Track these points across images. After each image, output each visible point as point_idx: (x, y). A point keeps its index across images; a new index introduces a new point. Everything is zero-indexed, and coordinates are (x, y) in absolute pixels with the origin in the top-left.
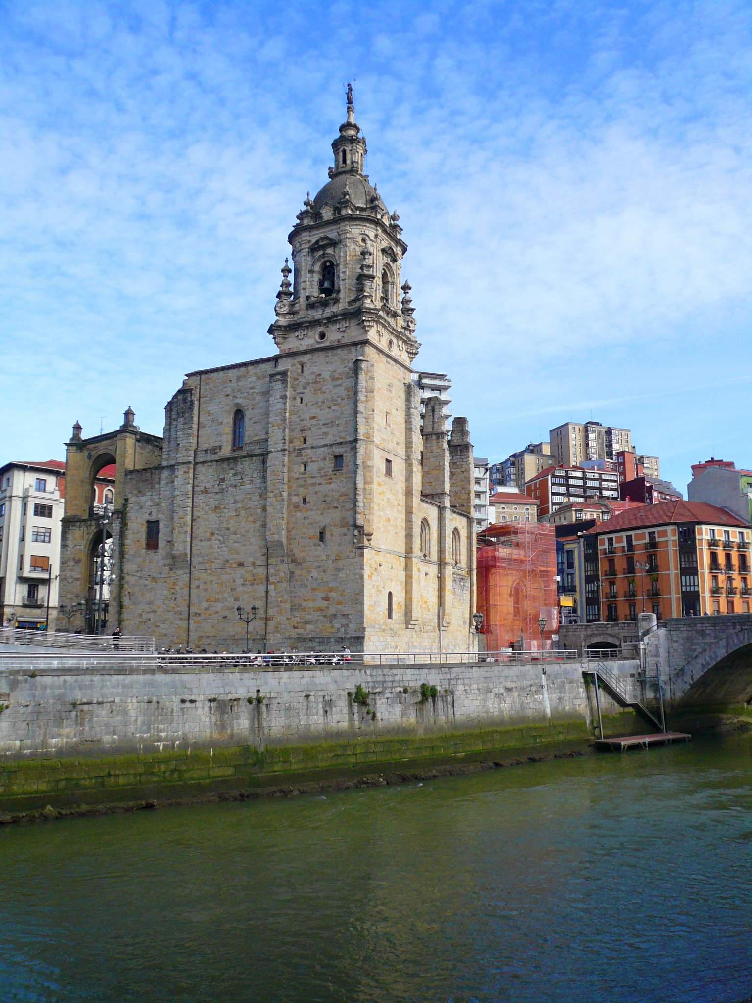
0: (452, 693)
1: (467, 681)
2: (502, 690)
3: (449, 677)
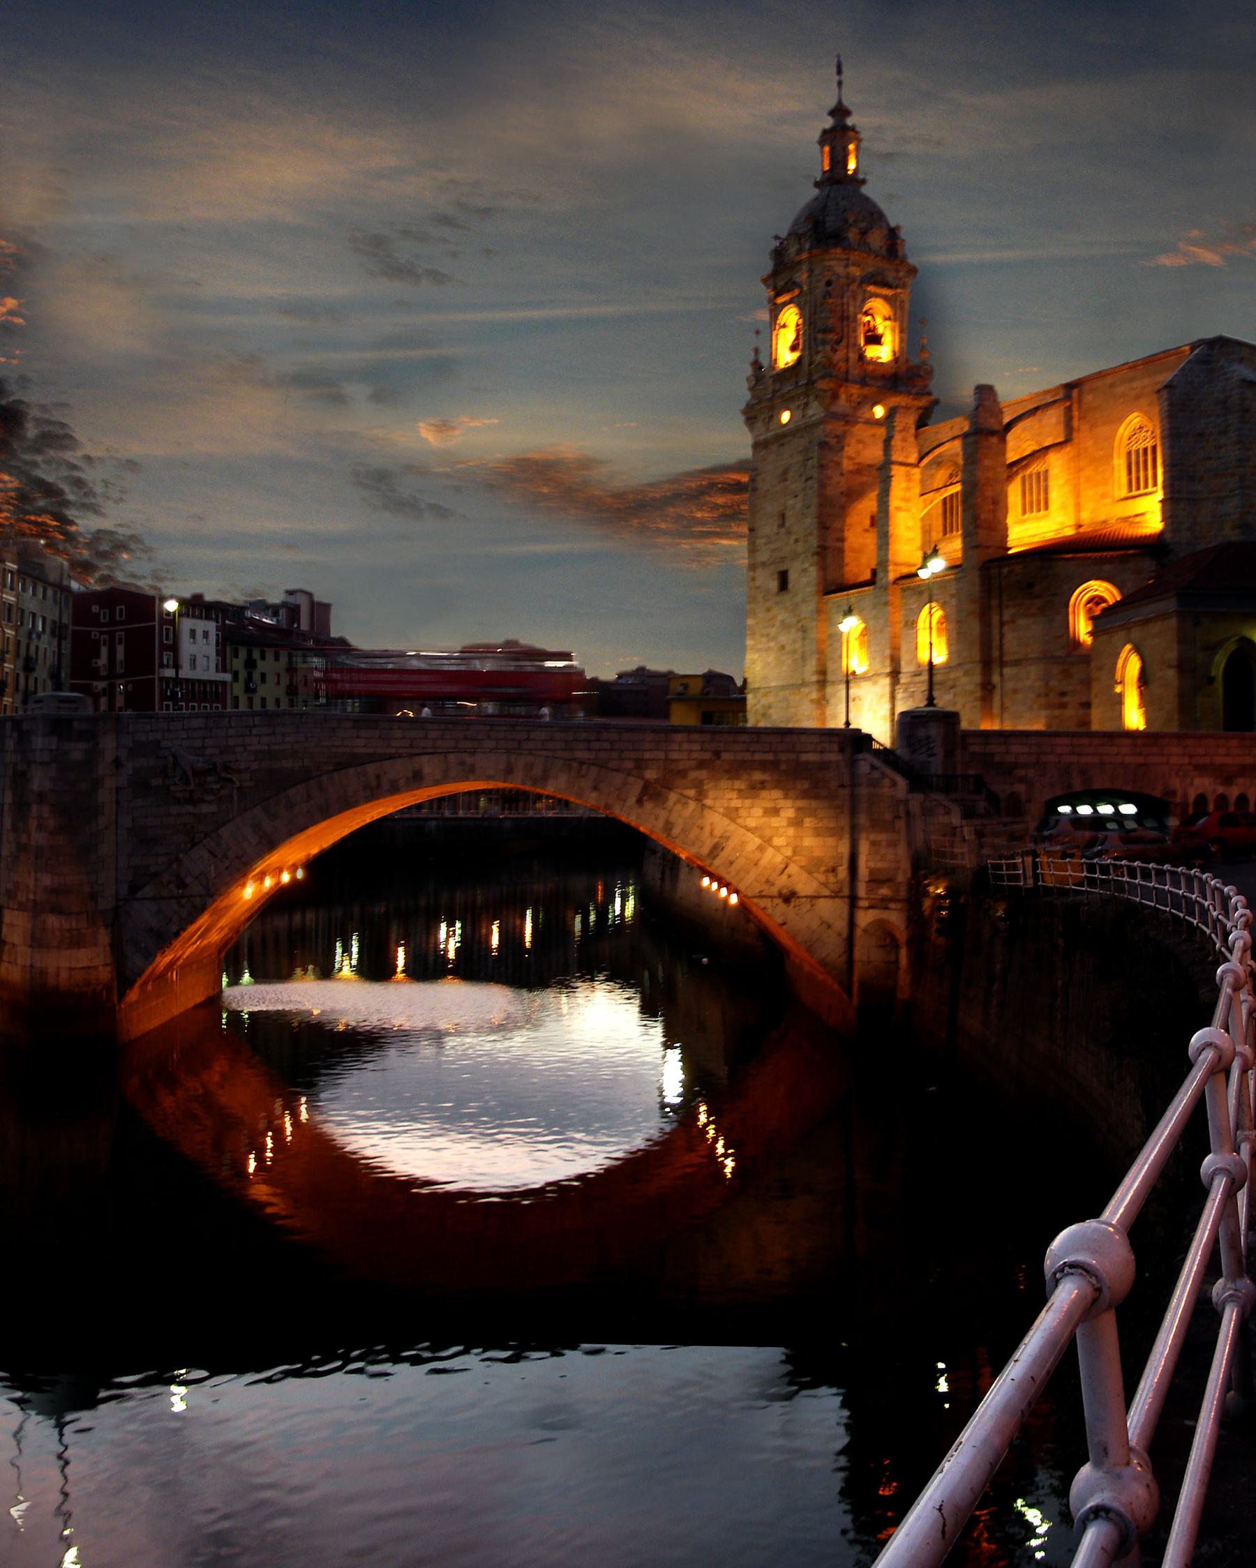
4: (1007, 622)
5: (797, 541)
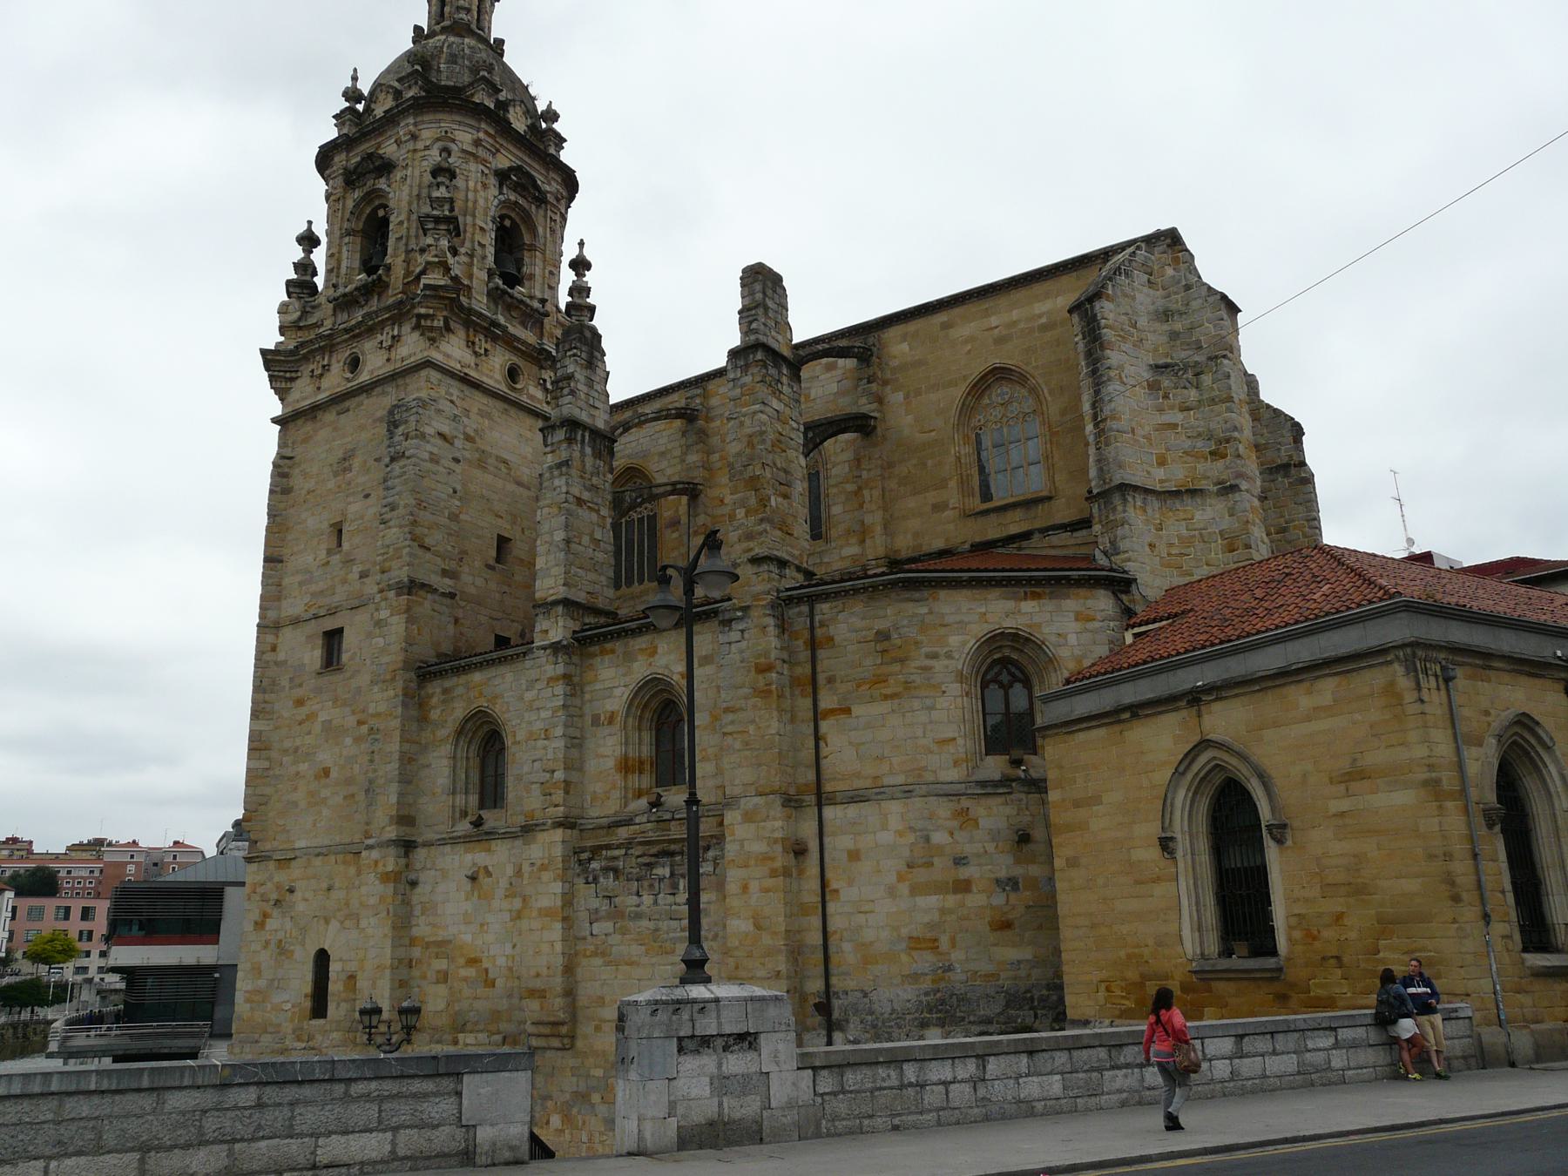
4: (832, 712)
5: (364, 575)
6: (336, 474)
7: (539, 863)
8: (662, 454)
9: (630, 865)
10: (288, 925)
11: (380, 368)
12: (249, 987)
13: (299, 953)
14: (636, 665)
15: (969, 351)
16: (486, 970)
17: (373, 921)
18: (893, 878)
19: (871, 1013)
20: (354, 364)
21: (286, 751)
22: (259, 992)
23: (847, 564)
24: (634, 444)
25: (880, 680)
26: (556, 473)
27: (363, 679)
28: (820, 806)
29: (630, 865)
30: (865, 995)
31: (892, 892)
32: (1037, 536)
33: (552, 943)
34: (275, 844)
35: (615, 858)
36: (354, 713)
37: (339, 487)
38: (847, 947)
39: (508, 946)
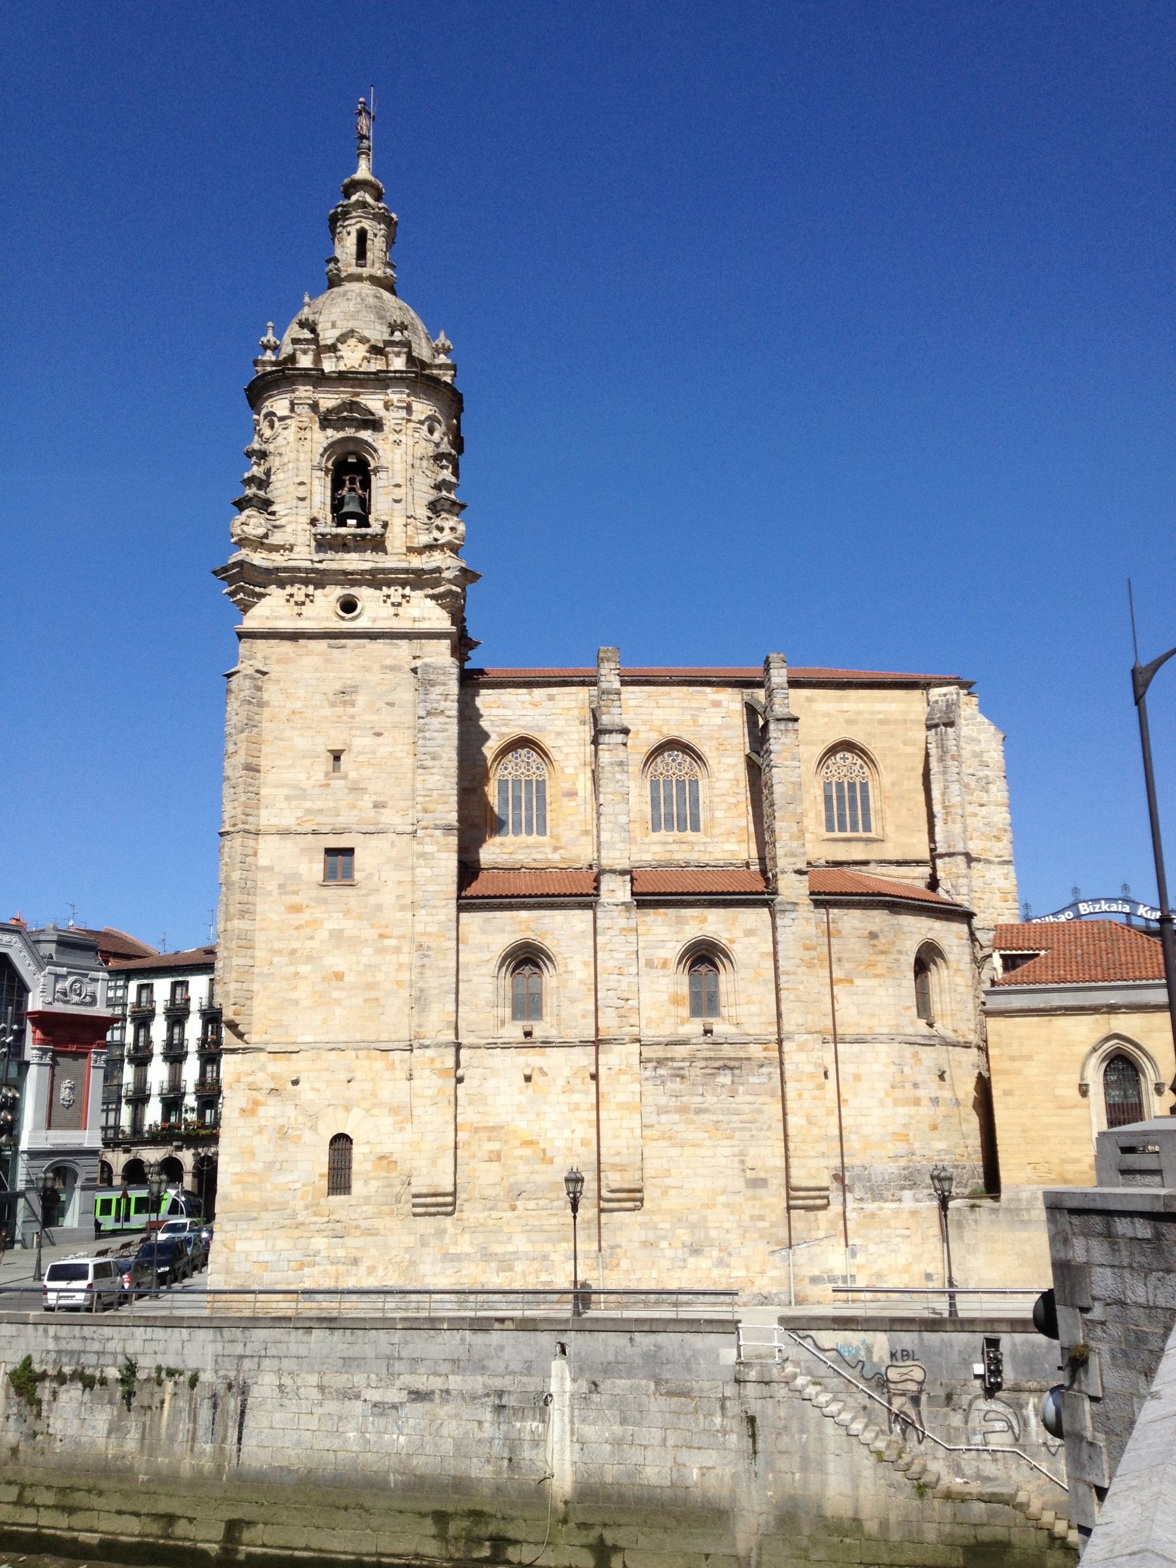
0: (244, 1391)
1: (287, 1364)
2: (394, 1395)
3: (239, 1349)
6: (333, 704)
7: (617, 1068)
8: (559, 734)
9: (695, 1072)
10: (291, 1111)
11: (386, 619)
12: (238, 1169)
13: (307, 1136)
14: (687, 928)
15: (826, 724)
16: (544, 1151)
17: (431, 1110)
18: (881, 1094)
19: (869, 1180)
20: (349, 606)
21: (278, 952)
22: (253, 1174)
23: (727, 856)
24: (529, 718)
25: (873, 965)
26: (617, 769)
27: (387, 898)
28: (835, 1043)
29: (695, 1072)
30: (866, 1169)
31: (882, 1104)
32: (872, 865)
33: (632, 1130)
34: (266, 1038)
35: (681, 1068)
36: (372, 926)
37: (338, 717)
38: (854, 1137)
39: (567, 1133)
